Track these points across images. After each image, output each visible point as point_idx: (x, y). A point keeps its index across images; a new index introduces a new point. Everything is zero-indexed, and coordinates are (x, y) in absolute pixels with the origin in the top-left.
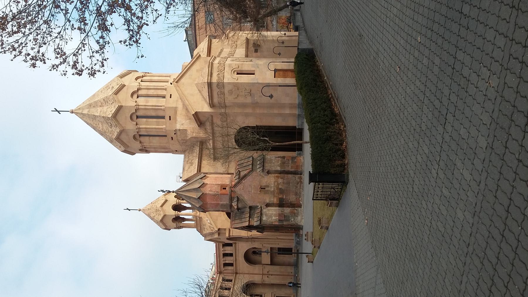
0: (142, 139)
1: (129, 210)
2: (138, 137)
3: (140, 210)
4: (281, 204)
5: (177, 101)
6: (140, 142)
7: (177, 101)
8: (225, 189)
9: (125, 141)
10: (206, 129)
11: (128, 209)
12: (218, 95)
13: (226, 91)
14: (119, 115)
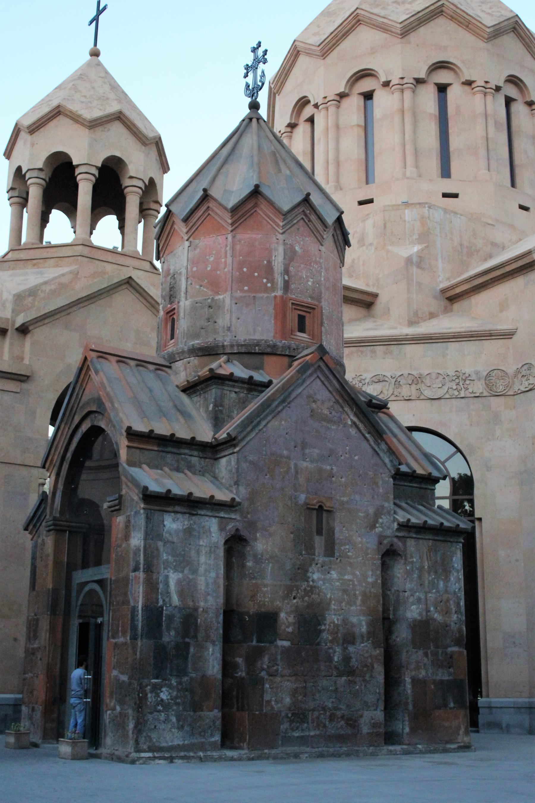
0: (354, 102)
1: (96, 19)
2: (366, 85)
4: (244, 626)
5: (512, 227)
6: (342, 96)
7: (512, 227)
8: (302, 329)
9: (345, 44)
10: (432, 316)
11: (100, 11)
14: (452, 26)
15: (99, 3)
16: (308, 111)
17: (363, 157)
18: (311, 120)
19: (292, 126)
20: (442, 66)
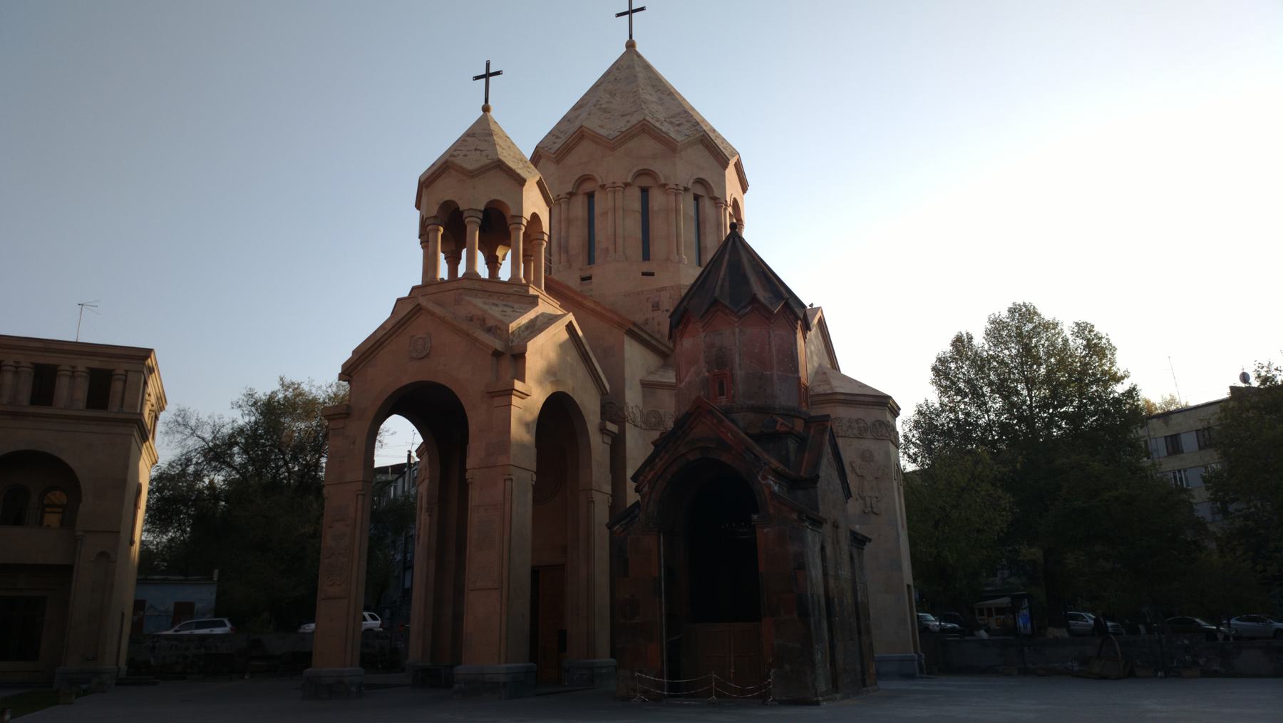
2: (645, 182)
3: (486, 109)
6: (627, 185)
9: (631, 144)
12: (858, 421)
13: (867, 444)
15: (488, 65)
16: (588, 187)
17: (640, 236)
18: (591, 196)
19: (571, 194)
20: (700, 181)
